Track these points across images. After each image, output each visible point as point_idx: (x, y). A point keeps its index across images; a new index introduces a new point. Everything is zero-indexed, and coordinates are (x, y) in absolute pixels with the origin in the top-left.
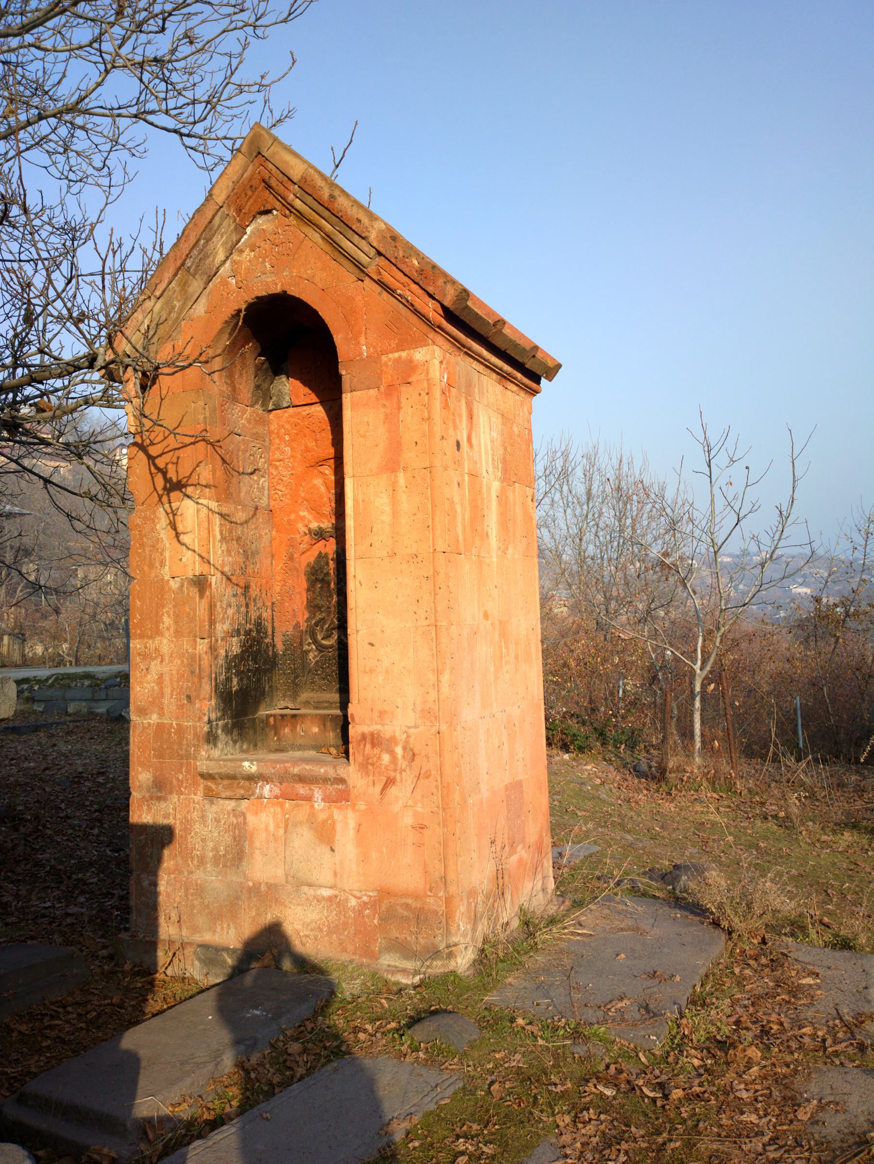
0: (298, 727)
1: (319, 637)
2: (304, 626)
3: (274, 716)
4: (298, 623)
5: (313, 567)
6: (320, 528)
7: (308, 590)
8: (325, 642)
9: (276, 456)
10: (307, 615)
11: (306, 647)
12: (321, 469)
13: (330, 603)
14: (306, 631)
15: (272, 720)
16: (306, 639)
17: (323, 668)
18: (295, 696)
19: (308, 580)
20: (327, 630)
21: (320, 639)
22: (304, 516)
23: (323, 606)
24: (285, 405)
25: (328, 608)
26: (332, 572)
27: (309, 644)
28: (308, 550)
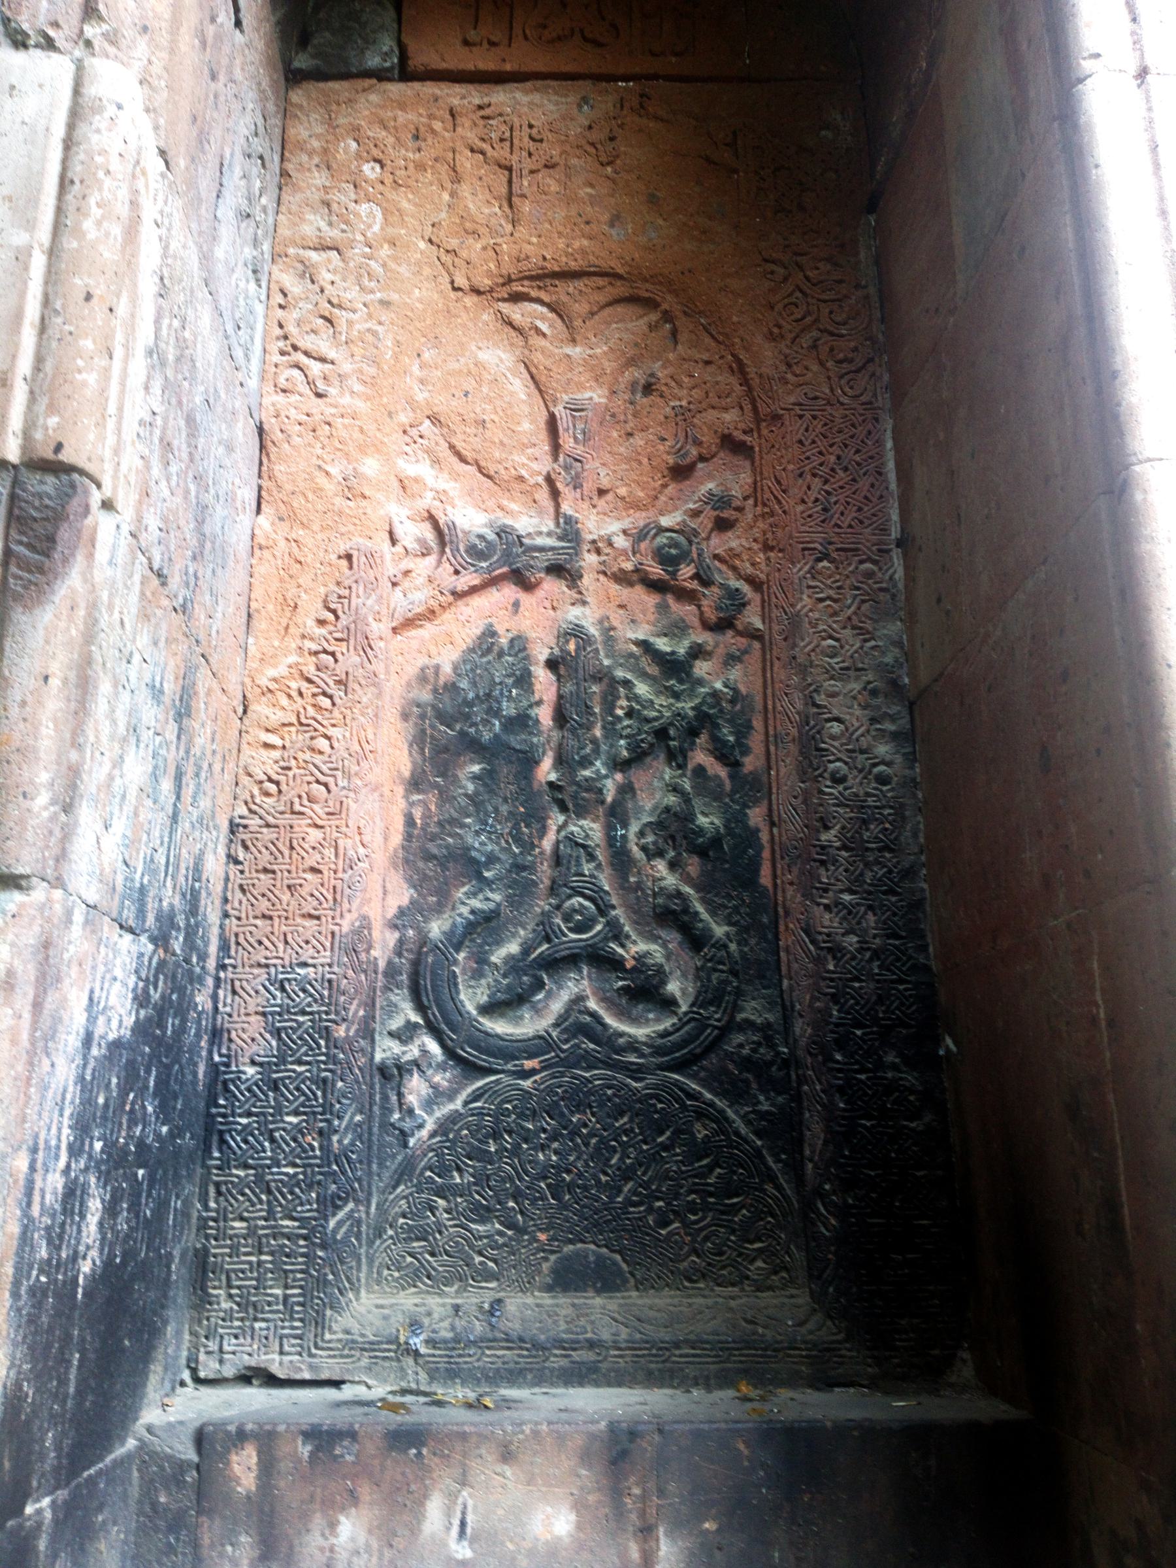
0: (434, 1508)
1: (471, 998)
2: (383, 946)
3: (265, 1438)
4: (365, 924)
5: (452, 688)
6: (503, 532)
7: (415, 784)
8: (499, 1027)
9: (308, 230)
10: (401, 895)
11: (386, 1049)
12: (516, 312)
13: (529, 846)
14: (391, 972)
15: (244, 1468)
17: (482, 1156)
18: (314, 1302)
19: (419, 740)
20: (514, 966)
21: (471, 1008)
23: (492, 859)
24: (373, 61)
25: (519, 867)
26: (545, 715)
27: (405, 1035)
28: (430, 614)
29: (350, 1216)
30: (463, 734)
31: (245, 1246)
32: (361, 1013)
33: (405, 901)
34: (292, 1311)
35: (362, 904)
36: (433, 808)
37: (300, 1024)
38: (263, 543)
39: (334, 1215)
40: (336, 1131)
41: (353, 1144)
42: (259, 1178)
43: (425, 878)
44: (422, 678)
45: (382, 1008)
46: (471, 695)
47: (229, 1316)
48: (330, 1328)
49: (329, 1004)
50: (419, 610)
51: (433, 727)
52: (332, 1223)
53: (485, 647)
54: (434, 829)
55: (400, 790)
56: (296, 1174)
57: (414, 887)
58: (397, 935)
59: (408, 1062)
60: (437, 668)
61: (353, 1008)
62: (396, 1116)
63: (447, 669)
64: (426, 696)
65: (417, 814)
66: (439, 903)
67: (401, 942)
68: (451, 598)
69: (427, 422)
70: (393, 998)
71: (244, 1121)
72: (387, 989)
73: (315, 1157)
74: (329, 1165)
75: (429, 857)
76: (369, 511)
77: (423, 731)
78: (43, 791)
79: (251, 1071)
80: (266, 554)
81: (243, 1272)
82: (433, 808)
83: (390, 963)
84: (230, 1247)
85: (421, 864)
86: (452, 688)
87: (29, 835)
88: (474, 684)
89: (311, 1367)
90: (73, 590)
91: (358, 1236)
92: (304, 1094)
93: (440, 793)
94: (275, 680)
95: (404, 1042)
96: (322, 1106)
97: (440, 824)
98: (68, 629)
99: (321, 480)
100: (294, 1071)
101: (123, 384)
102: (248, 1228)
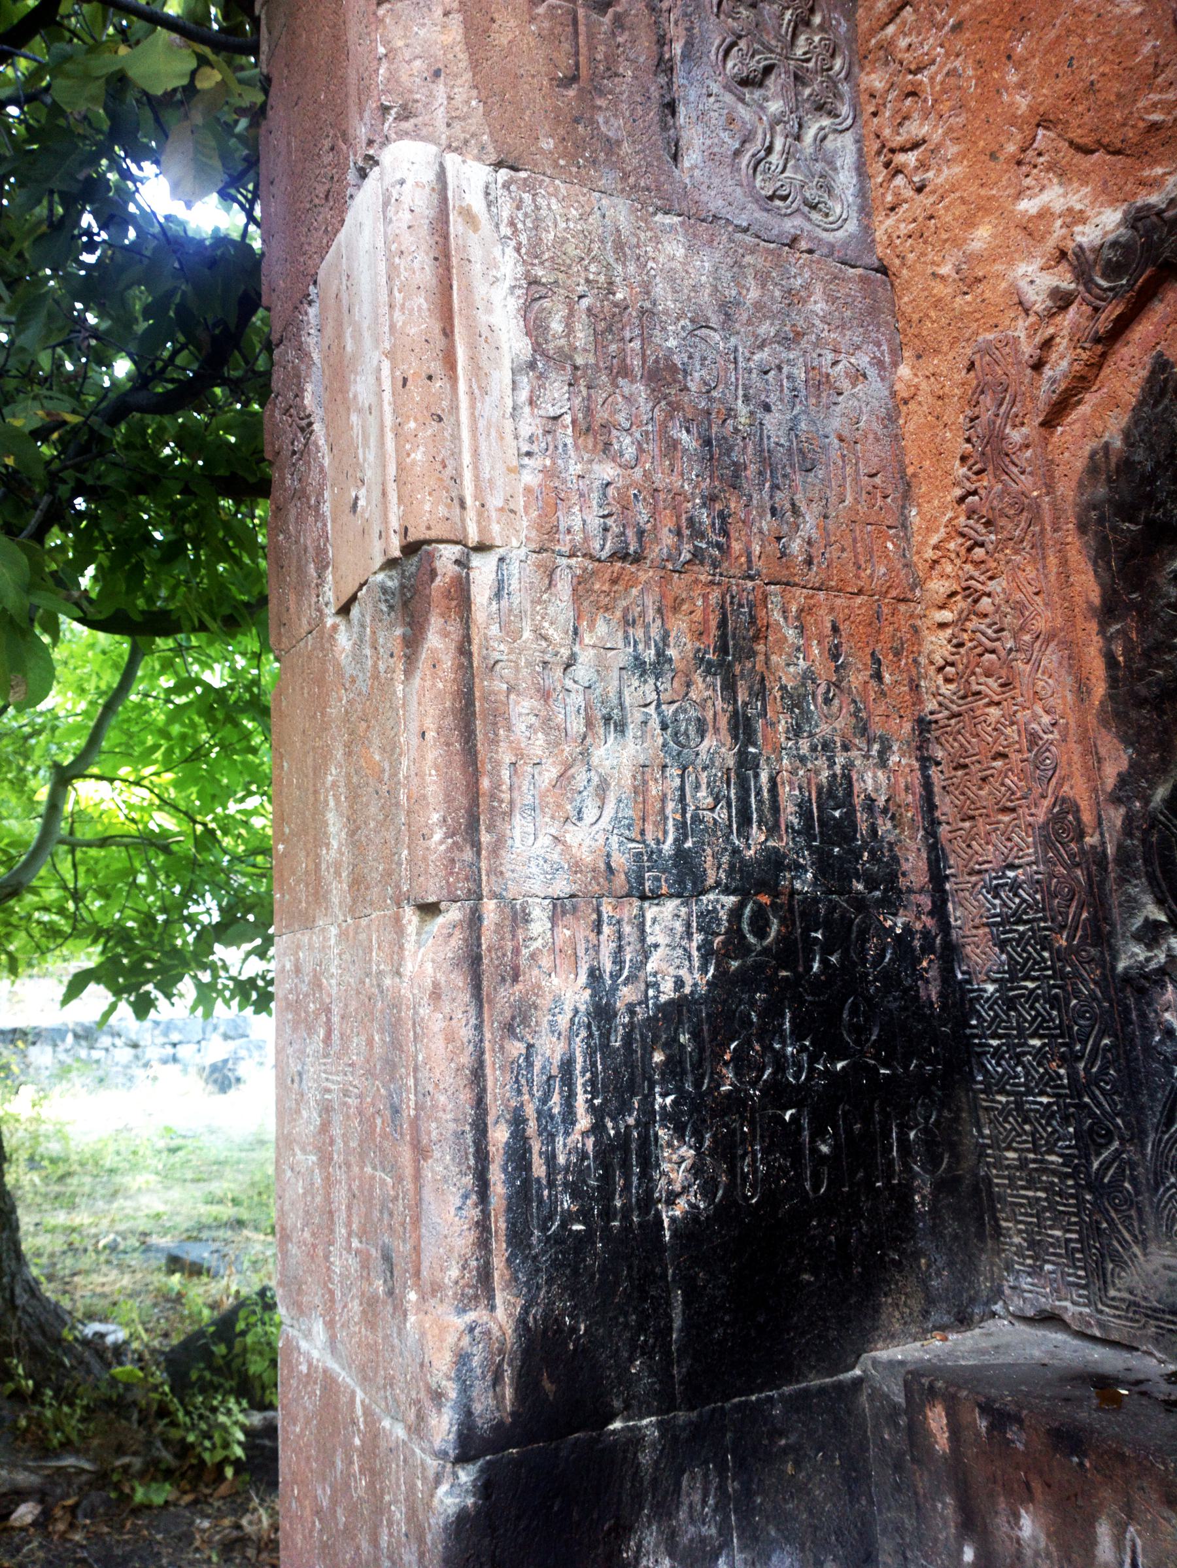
2: (1106, 828)
7: (1108, 611)
10: (1116, 762)
11: (1132, 955)
14: (1124, 857)
16: (1132, 905)
19: (1100, 555)
22: (1044, 214)
29: (1118, 1153)
30: (1149, 523)
31: (1021, 1179)
32: (1085, 915)
33: (1124, 765)
34: (1074, 1260)
35: (1060, 785)
36: (1134, 636)
37: (1022, 934)
38: (905, 395)
39: (1098, 1154)
40: (1079, 1059)
41: (1103, 1070)
42: (1019, 1105)
43: (1141, 731)
44: (1093, 469)
45: (1120, 905)
46: (1149, 466)
47: (1019, 1252)
48: (1114, 1284)
49: (1043, 910)
50: (1063, 386)
51: (1114, 529)
52: (1096, 1165)
53: (1157, 389)
54: (1138, 664)
55: (1093, 626)
56: (1050, 1104)
57: (1132, 745)
58: (1122, 810)
59: (1156, 971)
60: (1107, 446)
61: (1072, 910)
62: (1157, 1038)
63: (1118, 443)
64: (1102, 491)
65: (1118, 649)
66: (1162, 759)
67: (1129, 819)
68: (1100, 348)
69: (1041, 132)
70: (1133, 891)
71: (995, 1043)
72: (1122, 881)
73: (1062, 1086)
74: (1080, 1097)
75: (1141, 702)
76: (987, 294)
77: (1105, 538)
78: (437, 829)
79: (990, 988)
80: (912, 405)
81: (1022, 1205)
82: (1134, 636)
83: (1120, 847)
84: (1009, 1177)
85: (1133, 714)
86: (1127, 465)
87: (431, 869)
88: (1151, 448)
89: (1102, 1325)
90: (433, 651)
91: (1134, 1180)
92: (1039, 1014)
93: (1139, 613)
94: (935, 548)
95: (1149, 947)
96: (1059, 1027)
97: (1146, 655)
98: (434, 685)
99: (939, 289)
100: (1026, 988)
101: (474, 431)
102: (1019, 1159)
